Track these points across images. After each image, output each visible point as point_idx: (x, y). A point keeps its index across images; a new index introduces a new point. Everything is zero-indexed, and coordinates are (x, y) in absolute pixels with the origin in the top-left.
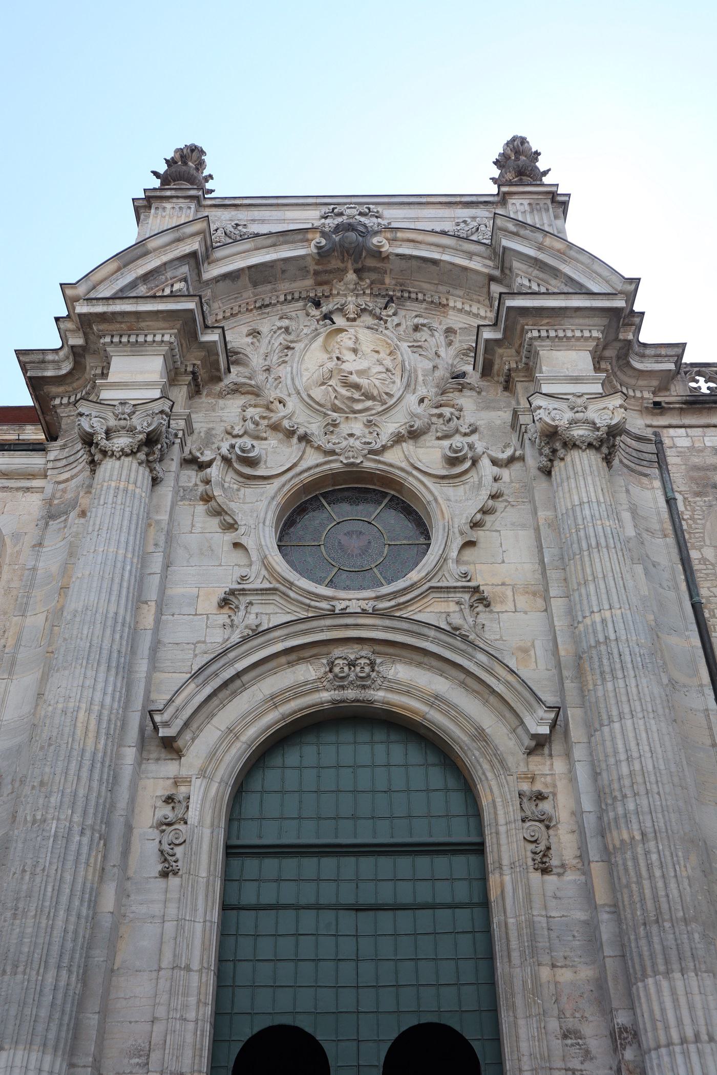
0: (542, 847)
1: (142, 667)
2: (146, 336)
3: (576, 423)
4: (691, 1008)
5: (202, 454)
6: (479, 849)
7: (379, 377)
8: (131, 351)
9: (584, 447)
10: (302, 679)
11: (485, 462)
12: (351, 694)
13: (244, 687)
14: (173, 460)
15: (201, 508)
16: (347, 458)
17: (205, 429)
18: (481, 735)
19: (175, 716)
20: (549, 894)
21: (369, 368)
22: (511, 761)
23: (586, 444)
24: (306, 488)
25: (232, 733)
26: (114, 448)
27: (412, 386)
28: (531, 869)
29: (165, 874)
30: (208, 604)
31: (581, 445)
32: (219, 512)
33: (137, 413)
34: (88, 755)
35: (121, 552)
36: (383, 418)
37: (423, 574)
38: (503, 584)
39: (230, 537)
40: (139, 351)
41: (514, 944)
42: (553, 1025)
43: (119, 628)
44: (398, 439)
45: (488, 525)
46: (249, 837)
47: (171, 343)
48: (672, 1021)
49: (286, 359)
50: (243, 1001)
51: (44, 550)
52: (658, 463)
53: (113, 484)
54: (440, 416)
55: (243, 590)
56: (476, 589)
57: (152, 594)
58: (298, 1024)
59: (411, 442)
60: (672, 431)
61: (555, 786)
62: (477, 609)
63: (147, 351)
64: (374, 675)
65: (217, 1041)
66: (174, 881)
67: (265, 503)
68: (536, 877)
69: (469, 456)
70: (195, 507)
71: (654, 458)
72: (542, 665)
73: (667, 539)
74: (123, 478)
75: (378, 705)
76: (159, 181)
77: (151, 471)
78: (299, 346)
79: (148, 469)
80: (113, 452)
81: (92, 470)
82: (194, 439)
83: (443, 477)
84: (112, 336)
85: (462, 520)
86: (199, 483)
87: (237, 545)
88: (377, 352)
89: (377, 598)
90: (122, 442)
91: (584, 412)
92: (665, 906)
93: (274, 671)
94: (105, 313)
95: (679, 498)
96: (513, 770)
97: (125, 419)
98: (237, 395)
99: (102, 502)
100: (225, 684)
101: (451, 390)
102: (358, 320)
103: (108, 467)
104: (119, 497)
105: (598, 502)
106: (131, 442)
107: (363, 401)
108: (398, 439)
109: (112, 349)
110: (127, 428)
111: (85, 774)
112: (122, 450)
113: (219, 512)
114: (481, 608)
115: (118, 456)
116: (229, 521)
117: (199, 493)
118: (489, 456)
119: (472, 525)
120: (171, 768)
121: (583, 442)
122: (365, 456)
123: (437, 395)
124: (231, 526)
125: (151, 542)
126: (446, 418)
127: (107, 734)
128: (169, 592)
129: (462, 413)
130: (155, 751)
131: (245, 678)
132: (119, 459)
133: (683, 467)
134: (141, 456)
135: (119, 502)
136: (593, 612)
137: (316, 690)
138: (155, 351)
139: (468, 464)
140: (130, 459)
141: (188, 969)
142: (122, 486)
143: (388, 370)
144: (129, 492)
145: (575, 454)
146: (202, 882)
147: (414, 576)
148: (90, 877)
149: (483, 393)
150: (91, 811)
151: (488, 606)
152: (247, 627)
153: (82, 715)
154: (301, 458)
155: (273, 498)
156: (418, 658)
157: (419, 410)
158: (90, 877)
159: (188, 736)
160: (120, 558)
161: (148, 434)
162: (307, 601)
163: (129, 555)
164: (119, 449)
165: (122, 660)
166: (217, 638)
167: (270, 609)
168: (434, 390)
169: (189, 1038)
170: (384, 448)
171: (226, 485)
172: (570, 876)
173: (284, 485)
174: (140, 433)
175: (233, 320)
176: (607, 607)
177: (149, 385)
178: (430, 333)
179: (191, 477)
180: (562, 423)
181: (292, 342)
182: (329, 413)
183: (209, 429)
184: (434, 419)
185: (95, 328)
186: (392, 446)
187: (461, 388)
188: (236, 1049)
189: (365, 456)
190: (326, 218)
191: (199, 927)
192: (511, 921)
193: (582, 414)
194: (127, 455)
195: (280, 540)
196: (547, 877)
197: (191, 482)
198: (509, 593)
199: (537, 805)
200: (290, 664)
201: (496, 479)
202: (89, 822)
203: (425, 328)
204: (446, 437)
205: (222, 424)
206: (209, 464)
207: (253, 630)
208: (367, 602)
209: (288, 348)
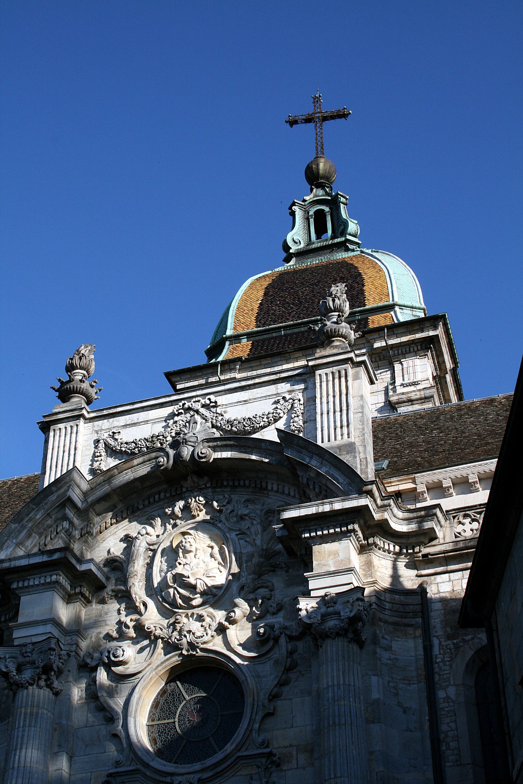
3: (329, 616)
9: (333, 637)
11: (283, 640)
23: (334, 634)
31: (331, 635)
37: (234, 746)
38: (291, 746)
52: (422, 612)
55: (117, 772)
62: (272, 770)
69: (272, 636)
73: (420, 684)
76: (58, 393)
77: (51, 690)
80: (22, 684)
89: (203, 770)
91: (333, 607)
95: (436, 642)
97: (28, 656)
101: (266, 572)
105: (339, 685)
110: (30, 662)
116: (108, 716)
118: (286, 634)
119: (271, 697)
123: (254, 580)
129: (273, 593)
133: (443, 612)
136: (325, 780)
139: (271, 643)
145: (329, 642)
147: (229, 748)
149: (290, 571)
151: (278, 765)
161: (43, 667)
162: (158, 778)
176: (332, 776)
178: (250, 521)
180: (315, 621)
187: (274, 568)
193: (333, 608)
198: (294, 753)
201: (291, 653)
203: (247, 518)
208: (192, 776)
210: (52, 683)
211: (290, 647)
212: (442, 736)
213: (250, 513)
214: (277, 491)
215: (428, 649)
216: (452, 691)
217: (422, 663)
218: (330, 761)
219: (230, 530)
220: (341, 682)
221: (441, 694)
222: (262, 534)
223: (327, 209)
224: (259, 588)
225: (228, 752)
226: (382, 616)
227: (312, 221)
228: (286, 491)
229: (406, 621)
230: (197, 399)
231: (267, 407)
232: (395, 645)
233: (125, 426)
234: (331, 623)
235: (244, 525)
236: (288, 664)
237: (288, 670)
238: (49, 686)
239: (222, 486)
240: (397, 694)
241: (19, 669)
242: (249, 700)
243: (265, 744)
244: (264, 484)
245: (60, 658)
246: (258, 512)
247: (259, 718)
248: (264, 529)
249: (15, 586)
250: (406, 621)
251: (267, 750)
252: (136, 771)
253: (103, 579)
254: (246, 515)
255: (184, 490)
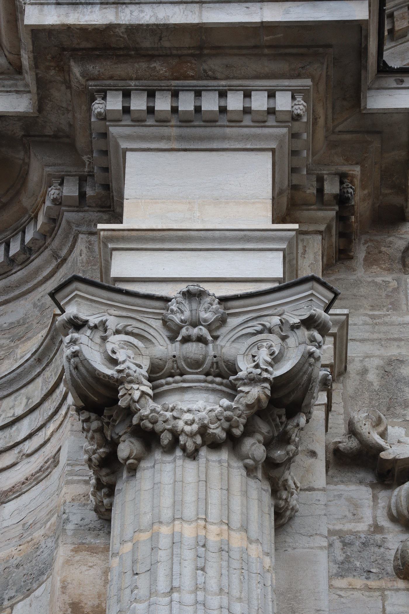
2: (223, 95)
5: (383, 435)
8: (181, 138)
14: (313, 454)
17: (377, 362)
26: (180, 424)
33: (233, 322)
40: (201, 139)
47: (296, 118)
63: (224, 138)
70: (384, 598)
74: (214, 513)
77: (275, 493)
79: (267, 487)
80: (175, 435)
81: (99, 486)
82: (350, 390)
84: (127, 95)
86: (384, 522)
94: (110, 27)
97: (201, 339)
99: (162, 585)
104: (212, 572)
106: (228, 408)
109: (127, 131)
110: (206, 366)
112: (203, 430)
115: (190, 446)
117: (391, 555)
132: (193, 455)
135: (213, 584)
138: (247, 138)
140: (224, 455)
142: (213, 539)
144: (236, 555)
164: (195, 427)
174: (252, 381)
177: (249, 240)
183: (390, 362)
185: (76, 70)
197: (360, 520)
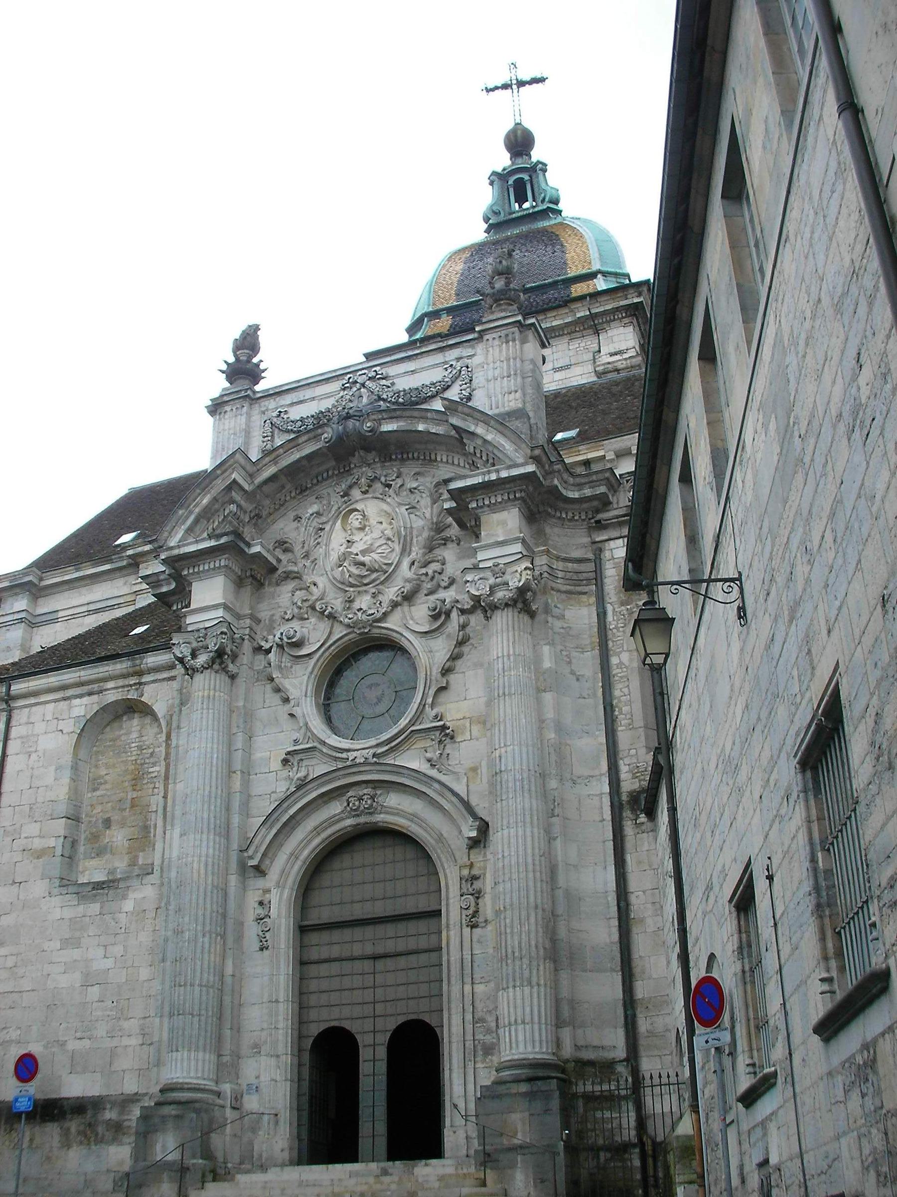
0: (471, 912)
1: (236, 820)
4: (515, 1007)
6: (437, 913)
7: (379, 551)
10: (333, 812)
11: (454, 614)
12: (362, 819)
13: (298, 824)
15: (269, 687)
16: (359, 629)
18: (440, 838)
19: (256, 852)
20: (475, 940)
21: (371, 545)
22: (458, 855)
24: (335, 656)
25: (294, 856)
27: (408, 550)
28: (464, 926)
29: (262, 949)
30: (276, 765)
32: (278, 690)
34: (202, 890)
35: (209, 745)
36: (386, 585)
37: (407, 721)
38: (464, 718)
39: (287, 708)
41: (453, 973)
42: (469, 1017)
43: (213, 800)
44: (395, 605)
45: (457, 668)
46: (314, 918)
48: (506, 1015)
49: (319, 540)
50: (313, 1015)
51: (182, 730)
53: (201, 694)
54: (427, 574)
56: (444, 728)
57: (238, 765)
58: (342, 1025)
59: (406, 603)
60: (612, 544)
61: (485, 868)
64: (375, 804)
65: (301, 1037)
66: (266, 952)
67: (306, 678)
68: (467, 931)
71: (593, 575)
72: (485, 780)
74: (206, 687)
75: (381, 824)
78: (327, 527)
83: (426, 633)
85: (436, 671)
87: (292, 715)
88: (381, 523)
89: (378, 745)
90: (202, 659)
92: (510, 951)
93: (317, 809)
95: (609, 608)
96: (458, 862)
98: (289, 580)
100: (285, 824)
102: (371, 490)
103: (199, 678)
107: (369, 575)
108: (395, 605)
111: (201, 901)
113: (278, 690)
114: (448, 740)
120: (261, 883)
121: (501, 604)
122: (371, 625)
123: (425, 554)
124: (286, 700)
125: (234, 724)
126: (430, 577)
127: (213, 874)
128: (253, 757)
130: (251, 872)
131: (298, 818)
132: (202, 672)
134: (216, 667)
137: (343, 819)
139: (443, 617)
141: (277, 1001)
143: (389, 539)
145: (498, 613)
146: (282, 951)
148: (212, 959)
149: (462, 543)
150: (208, 921)
151: (452, 738)
152: (298, 779)
153: (195, 865)
154: (330, 633)
155: (311, 673)
156: (403, 788)
157: (409, 575)
158: (212, 959)
159: (267, 862)
160: (209, 750)
161: (216, 651)
162: (334, 754)
163: (215, 746)
165: (218, 822)
166: (283, 788)
167: (314, 761)
168: (421, 551)
169: (281, 1038)
170: (385, 615)
171: (283, 665)
172: (490, 927)
173: (318, 660)
175: (283, 508)
176: (502, 745)
179: (260, 661)
180: (484, 592)
181: (323, 524)
182: (347, 589)
184: (423, 578)
186: (392, 610)
187: (446, 541)
188: (311, 1040)
189: (371, 625)
190: (344, 389)
191: (282, 977)
192: (452, 959)
194: (207, 668)
195: (327, 698)
196: (474, 930)
198: (468, 725)
199: (472, 884)
200: (326, 803)
201: (463, 627)
202: (207, 928)
204: (431, 593)
205: (280, 610)
206: (268, 651)
207: (303, 781)
208: (367, 751)
209: (321, 529)
210: (227, 666)
211: (461, 621)
212: (615, 702)
213: (419, 486)
214: (447, 462)
215: (602, 615)
216: (625, 657)
217: (596, 630)
218: (499, 731)
219: (400, 504)
220: (511, 652)
221: (614, 660)
222: (432, 507)
223: (526, 178)
224: (430, 563)
225: (402, 727)
226: (554, 585)
227: (511, 190)
228: (456, 462)
229: (579, 589)
230: (363, 372)
231: (436, 375)
232: (568, 614)
233: (292, 404)
234: (500, 594)
235: (413, 499)
236: (460, 638)
237: (460, 643)
238: (225, 670)
239: (391, 459)
240: (570, 663)
241: (194, 655)
242: (421, 676)
243: (438, 717)
244: (433, 457)
245: (234, 642)
246: (428, 485)
247: (432, 692)
248: (434, 502)
249: (185, 572)
250: (579, 589)
251: (441, 723)
252: (313, 749)
253: (274, 562)
254: (415, 489)
255: (352, 466)
